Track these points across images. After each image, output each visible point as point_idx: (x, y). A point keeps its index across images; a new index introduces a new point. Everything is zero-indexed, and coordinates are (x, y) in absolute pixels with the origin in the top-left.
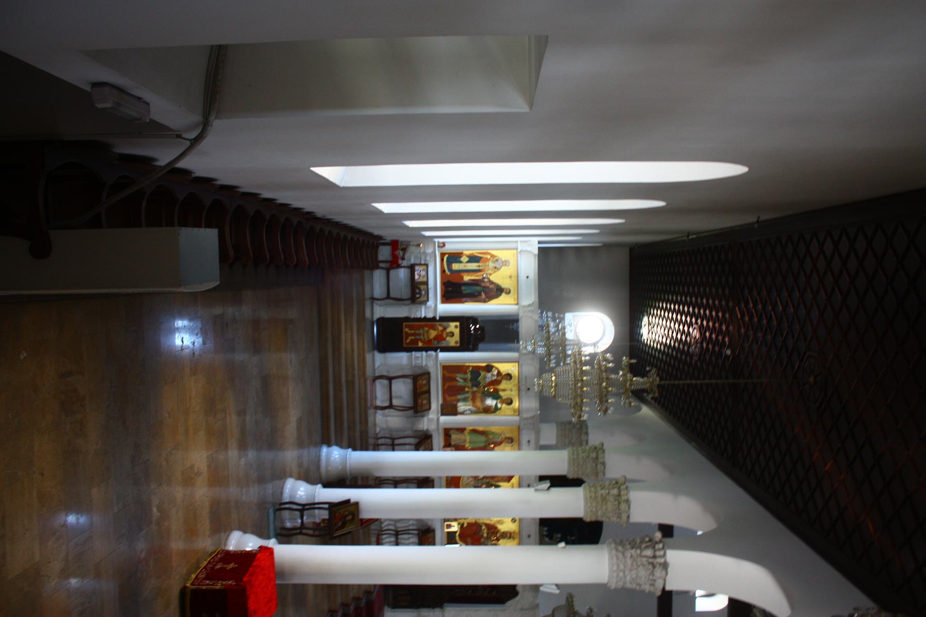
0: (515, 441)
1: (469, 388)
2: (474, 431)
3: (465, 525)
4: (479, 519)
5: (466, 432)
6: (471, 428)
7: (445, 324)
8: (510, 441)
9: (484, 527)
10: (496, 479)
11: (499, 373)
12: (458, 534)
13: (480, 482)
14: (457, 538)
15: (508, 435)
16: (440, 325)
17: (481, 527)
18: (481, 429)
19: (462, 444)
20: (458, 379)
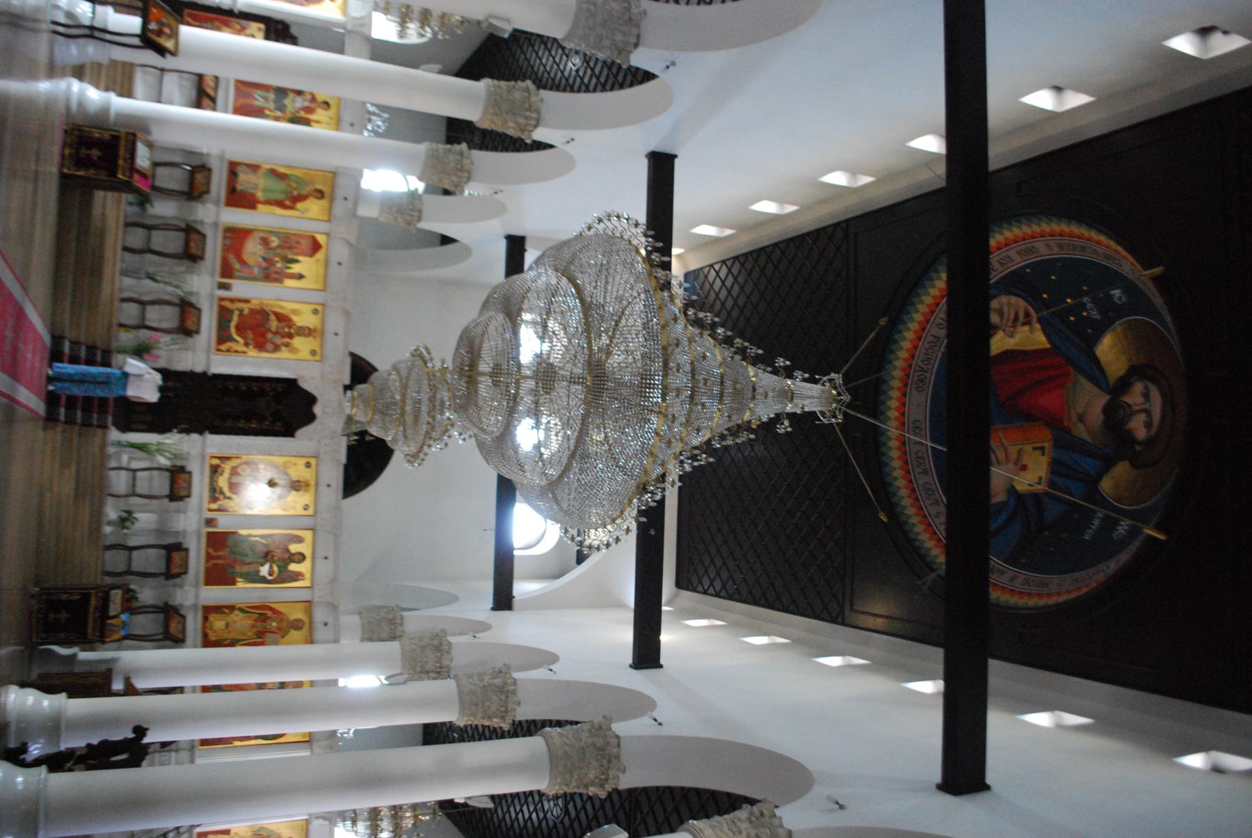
0: (327, 195)
1: (270, 110)
2: (273, 173)
3: (246, 312)
4: (267, 305)
5: (261, 172)
6: (269, 167)
7: (244, 23)
8: (319, 195)
9: (273, 317)
10: (295, 251)
11: (313, 99)
12: (233, 324)
13: (271, 251)
14: (233, 330)
15: (320, 187)
16: (238, 23)
17: (268, 315)
18: (282, 170)
19: (253, 191)
20: (257, 97)
